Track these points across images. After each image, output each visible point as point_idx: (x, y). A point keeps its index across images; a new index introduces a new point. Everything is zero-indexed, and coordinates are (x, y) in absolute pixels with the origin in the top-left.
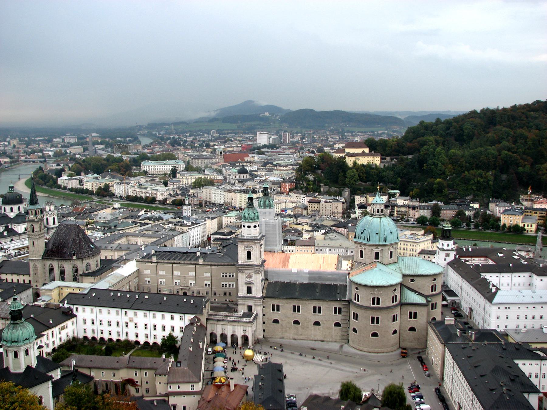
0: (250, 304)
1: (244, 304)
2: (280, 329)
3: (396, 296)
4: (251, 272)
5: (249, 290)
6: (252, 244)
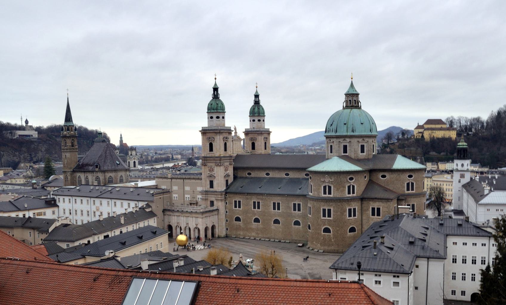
0: (213, 199)
3: (353, 187)
4: (213, 165)
5: (212, 186)
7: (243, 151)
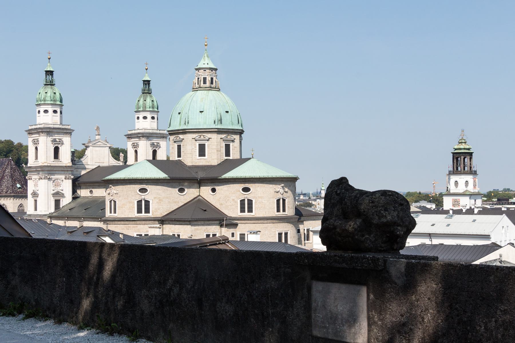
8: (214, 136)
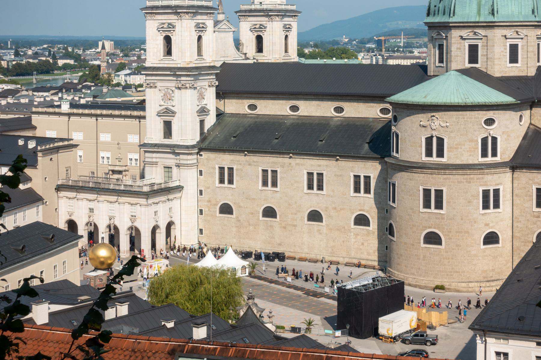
1: (156, 163)
2: (234, 229)
3: (494, 139)
6: (172, 19)
7: (237, 56)
8: (531, 32)
